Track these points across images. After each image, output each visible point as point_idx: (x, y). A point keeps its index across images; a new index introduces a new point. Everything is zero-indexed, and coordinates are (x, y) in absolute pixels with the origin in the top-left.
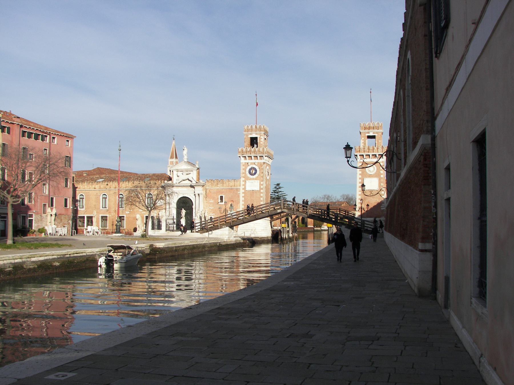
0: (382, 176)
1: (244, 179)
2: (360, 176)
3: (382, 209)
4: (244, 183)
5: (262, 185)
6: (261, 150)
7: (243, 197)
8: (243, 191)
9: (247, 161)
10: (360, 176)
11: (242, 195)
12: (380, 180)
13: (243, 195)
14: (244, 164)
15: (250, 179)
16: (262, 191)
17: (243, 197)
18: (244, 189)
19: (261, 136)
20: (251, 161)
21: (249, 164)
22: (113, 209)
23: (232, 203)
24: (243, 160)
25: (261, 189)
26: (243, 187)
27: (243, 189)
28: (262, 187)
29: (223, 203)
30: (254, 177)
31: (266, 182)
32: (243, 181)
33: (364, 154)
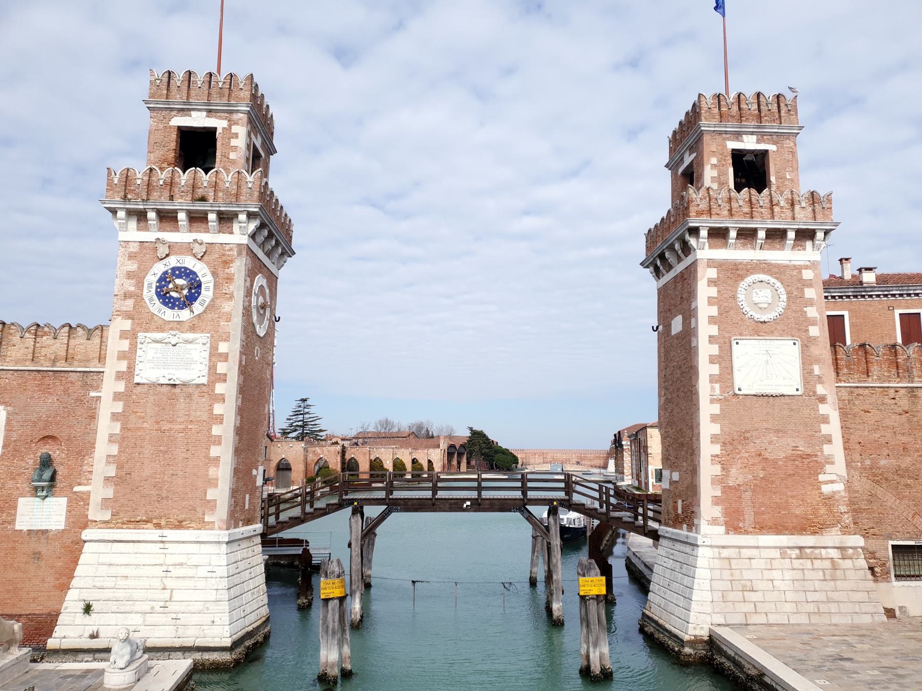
0: (814, 331)
1: (127, 325)
2: (714, 330)
3: (826, 489)
4: (125, 345)
5: (225, 357)
6: (228, 179)
7: (115, 417)
9: (150, 236)
10: (714, 330)
12: (805, 348)
13: (119, 407)
14: (134, 248)
16: (220, 388)
17: (115, 417)
18: (127, 375)
19: (232, 123)
20: (171, 237)
21: (162, 250)
24: (132, 233)
25: (216, 377)
26: (123, 366)
27: (119, 376)
28: (221, 368)
31: (247, 349)
32: (123, 335)
33: (733, 226)
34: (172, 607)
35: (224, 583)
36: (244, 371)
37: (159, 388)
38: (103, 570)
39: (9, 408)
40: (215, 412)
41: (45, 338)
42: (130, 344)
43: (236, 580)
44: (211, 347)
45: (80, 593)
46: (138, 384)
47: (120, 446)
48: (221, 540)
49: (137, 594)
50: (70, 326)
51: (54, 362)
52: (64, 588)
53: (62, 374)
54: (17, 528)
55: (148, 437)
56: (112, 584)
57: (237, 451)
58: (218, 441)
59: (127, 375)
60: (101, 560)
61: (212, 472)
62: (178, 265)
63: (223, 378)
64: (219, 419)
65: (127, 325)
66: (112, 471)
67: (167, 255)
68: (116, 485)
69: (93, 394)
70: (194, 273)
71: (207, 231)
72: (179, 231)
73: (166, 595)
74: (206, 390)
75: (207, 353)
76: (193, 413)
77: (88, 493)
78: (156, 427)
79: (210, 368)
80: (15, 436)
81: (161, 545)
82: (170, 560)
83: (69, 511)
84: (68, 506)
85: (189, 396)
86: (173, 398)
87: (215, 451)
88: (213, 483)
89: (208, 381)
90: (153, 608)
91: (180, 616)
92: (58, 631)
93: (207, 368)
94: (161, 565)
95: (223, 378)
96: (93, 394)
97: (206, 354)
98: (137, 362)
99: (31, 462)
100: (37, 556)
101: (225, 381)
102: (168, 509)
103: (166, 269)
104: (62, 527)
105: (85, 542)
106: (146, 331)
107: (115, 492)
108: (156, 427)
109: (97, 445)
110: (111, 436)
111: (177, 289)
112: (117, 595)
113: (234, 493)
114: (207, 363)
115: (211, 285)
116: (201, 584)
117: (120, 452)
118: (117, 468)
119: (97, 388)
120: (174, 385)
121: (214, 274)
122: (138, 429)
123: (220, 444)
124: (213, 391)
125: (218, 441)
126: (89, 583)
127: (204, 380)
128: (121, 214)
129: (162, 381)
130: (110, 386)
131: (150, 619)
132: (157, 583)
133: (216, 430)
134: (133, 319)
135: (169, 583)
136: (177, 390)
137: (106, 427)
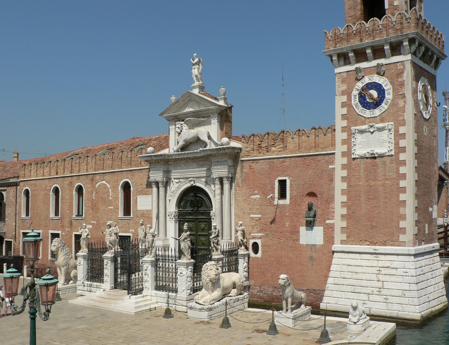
1: (345, 123)
4: (345, 136)
5: (403, 136)
7: (343, 179)
8: (345, 161)
11: (340, 173)
13: (345, 173)
15: (364, 120)
16: (402, 157)
17: (343, 179)
20: (364, 65)
22: (68, 219)
23: (310, 200)
26: (345, 148)
27: (344, 154)
28: (402, 143)
29: (287, 201)
30: (377, 112)
31: (418, 129)
32: (344, 129)
34: (384, 292)
35: (414, 280)
36: (418, 143)
37: (366, 160)
38: (345, 268)
39: (291, 178)
40: (401, 172)
41: (303, 137)
42: (348, 135)
43: (422, 278)
44: (395, 131)
45: (334, 280)
46: (354, 159)
47: (348, 197)
48: (410, 253)
49: (364, 283)
50: (315, 129)
51: (310, 149)
52: (327, 277)
53: (314, 157)
54: (301, 243)
55: (362, 190)
56: (350, 277)
57: (417, 196)
58: (403, 190)
59: (347, 154)
60: (344, 263)
61: (401, 210)
62: (370, 81)
63: (403, 150)
64: (404, 176)
65: (345, 123)
66: (344, 211)
67: (363, 77)
68: (348, 219)
69: (331, 167)
70: (380, 85)
71: (384, 56)
72: (368, 60)
73: (380, 284)
74: (395, 159)
75: (393, 135)
76: (387, 174)
77: (333, 224)
78: (366, 184)
79: (395, 144)
80: (295, 193)
81: (376, 256)
82: (381, 264)
83: (325, 234)
84: (324, 232)
85: (384, 163)
86: (375, 165)
87: (402, 197)
88: (403, 217)
89: (395, 153)
90: (373, 291)
91: (388, 297)
92: (325, 300)
93: (393, 144)
94: (376, 267)
95: (403, 150)
96: (331, 167)
97: (392, 136)
98: (353, 146)
99: (304, 207)
100: (311, 258)
101: (405, 151)
102: (377, 234)
103: (363, 85)
104: (322, 243)
105: (334, 252)
106: (356, 125)
107: (348, 223)
108: (366, 184)
109: (335, 197)
110: (342, 190)
111: (371, 96)
112: (353, 283)
113: (417, 223)
114: (393, 141)
115: (391, 91)
116: (400, 279)
117: (347, 200)
118: (347, 210)
119: (332, 163)
120: (375, 158)
121: (391, 83)
122: (356, 186)
123: (405, 192)
124: (398, 158)
125: (403, 190)
126: (338, 274)
127: (393, 153)
128: (335, 58)
129: (368, 156)
130: (340, 160)
131: (372, 297)
132: (374, 277)
133: (402, 184)
134: (347, 119)
135: (381, 278)
136: (377, 160)
137: (339, 186)
